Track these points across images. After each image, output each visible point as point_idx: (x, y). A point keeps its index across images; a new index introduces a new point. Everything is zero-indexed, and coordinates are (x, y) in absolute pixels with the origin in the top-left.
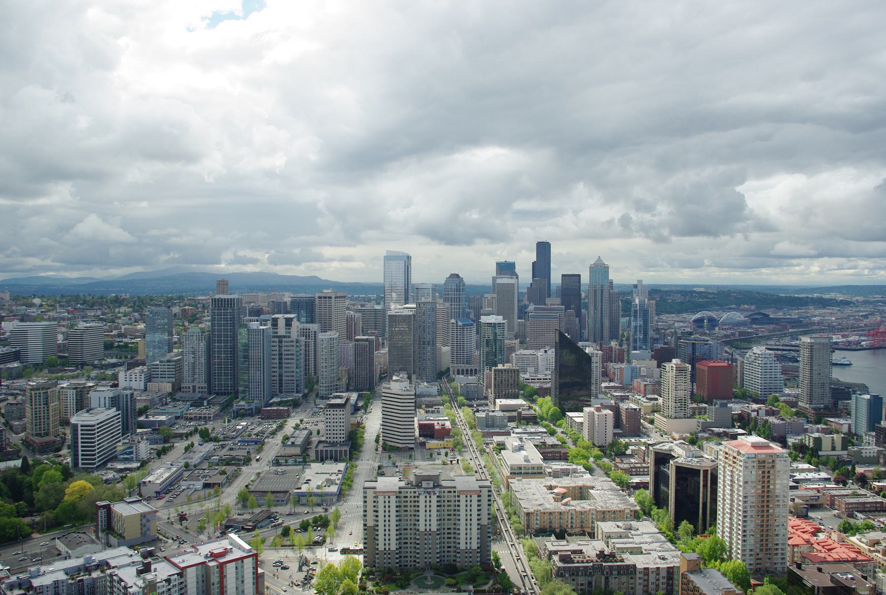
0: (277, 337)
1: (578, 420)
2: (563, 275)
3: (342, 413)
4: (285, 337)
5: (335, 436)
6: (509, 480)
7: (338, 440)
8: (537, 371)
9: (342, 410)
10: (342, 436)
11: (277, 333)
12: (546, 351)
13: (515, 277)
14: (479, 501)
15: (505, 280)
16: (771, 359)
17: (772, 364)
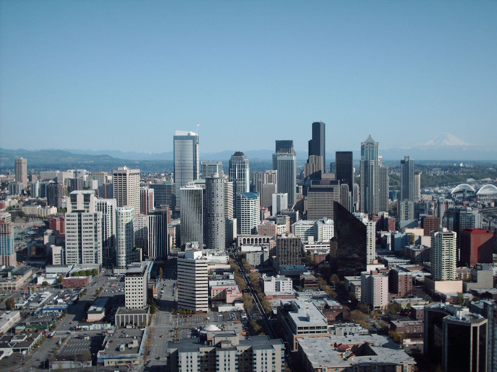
0: (76, 211)
1: (355, 283)
2: (338, 153)
3: (140, 281)
4: (83, 211)
5: (134, 302)
6: (299, 340)
7: (138, 306)
8: (316, 239)
9: (140, 278)
10: (141, 302)
11: (76, 208)
12: (323, 222)
13: (293, 154)
14: (273, 358)
15: (284, 157)
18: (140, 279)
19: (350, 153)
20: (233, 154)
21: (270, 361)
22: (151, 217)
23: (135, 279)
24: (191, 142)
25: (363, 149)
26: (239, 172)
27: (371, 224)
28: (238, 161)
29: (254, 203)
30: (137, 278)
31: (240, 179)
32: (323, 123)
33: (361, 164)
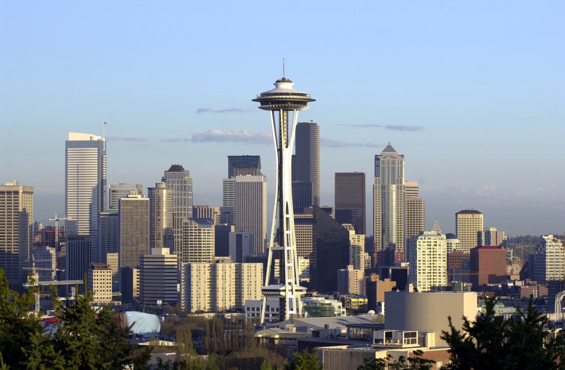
2: (338, 176)
3: (109, 274)
9: (109, 271)
16: (557, 247)
17: (558, 252)
18: (109, 272)
19: (362, 176)
20: (168, 170)
21: (253, 271)
22: (72, 243)
23: (104, 272)
24: (94, 151)
25: (377, 166)
26: (177, 197)
27: (359, 236)
28: (177, 180)
29: (208, 233)
30: (106, 271)
31: (180, 207)
32: (316, 124)
33: (375, 191)
